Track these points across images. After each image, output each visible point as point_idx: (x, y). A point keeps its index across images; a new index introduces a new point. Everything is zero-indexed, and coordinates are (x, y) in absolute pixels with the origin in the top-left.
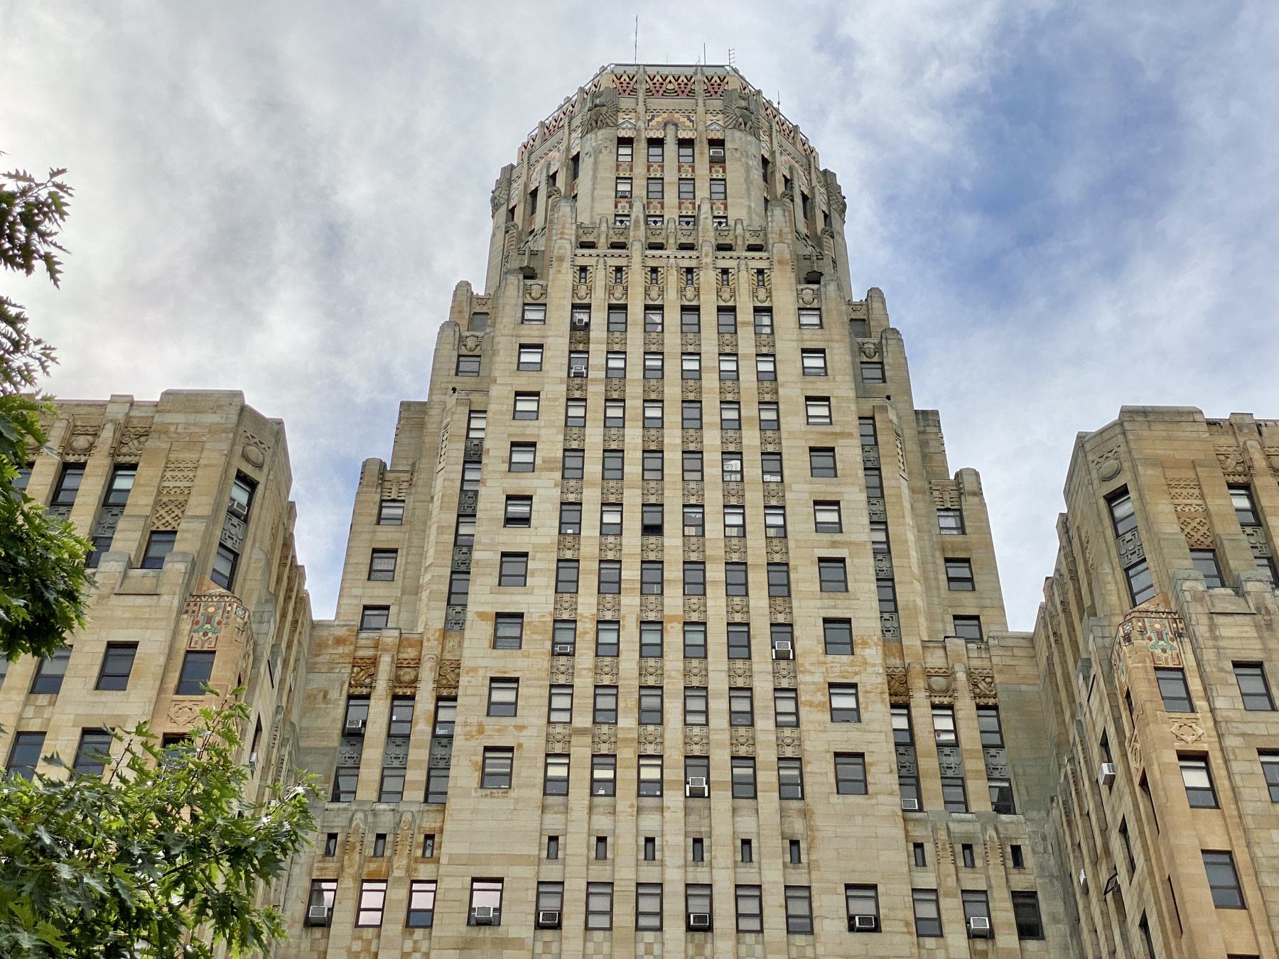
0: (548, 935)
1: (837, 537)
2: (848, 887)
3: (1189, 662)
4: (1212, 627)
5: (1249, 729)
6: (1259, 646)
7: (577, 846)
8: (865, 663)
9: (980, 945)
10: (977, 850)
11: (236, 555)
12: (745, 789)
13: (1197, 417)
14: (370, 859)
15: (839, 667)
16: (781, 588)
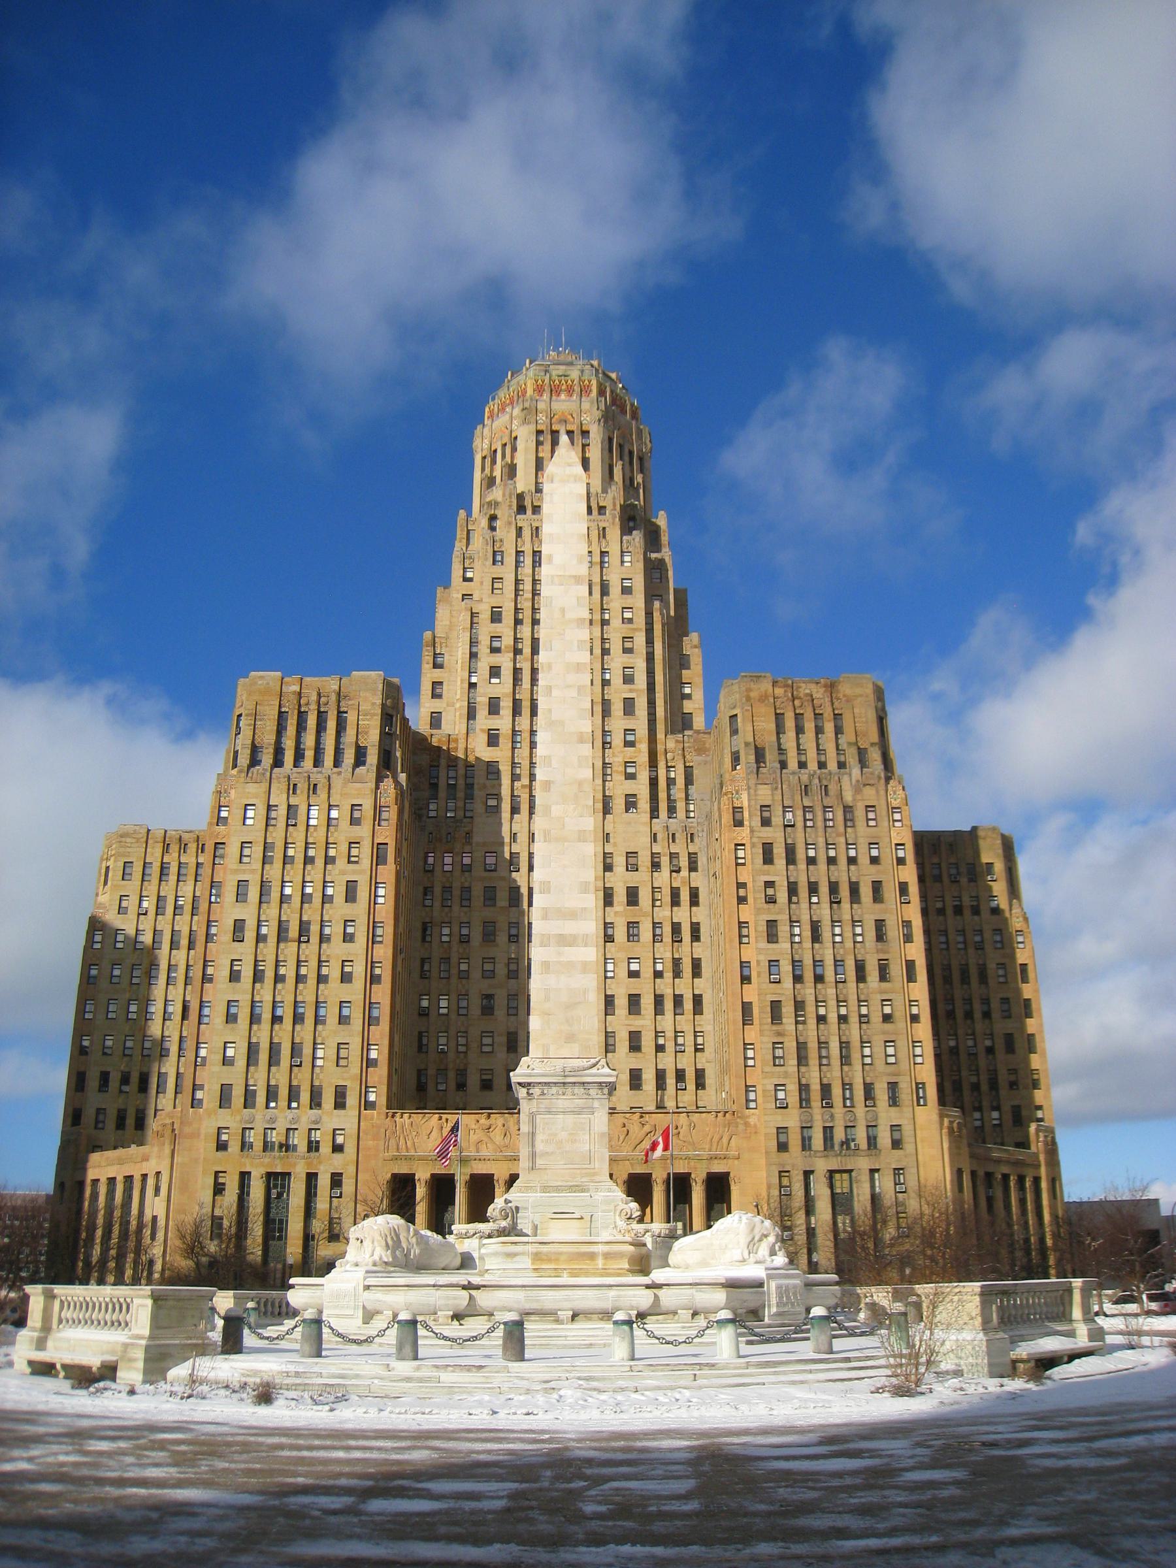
2: (627, 853)
3: (745, 804)
5: (761, 835)
6: (770, 797)
8: (640, 751)
10: (677, 835)
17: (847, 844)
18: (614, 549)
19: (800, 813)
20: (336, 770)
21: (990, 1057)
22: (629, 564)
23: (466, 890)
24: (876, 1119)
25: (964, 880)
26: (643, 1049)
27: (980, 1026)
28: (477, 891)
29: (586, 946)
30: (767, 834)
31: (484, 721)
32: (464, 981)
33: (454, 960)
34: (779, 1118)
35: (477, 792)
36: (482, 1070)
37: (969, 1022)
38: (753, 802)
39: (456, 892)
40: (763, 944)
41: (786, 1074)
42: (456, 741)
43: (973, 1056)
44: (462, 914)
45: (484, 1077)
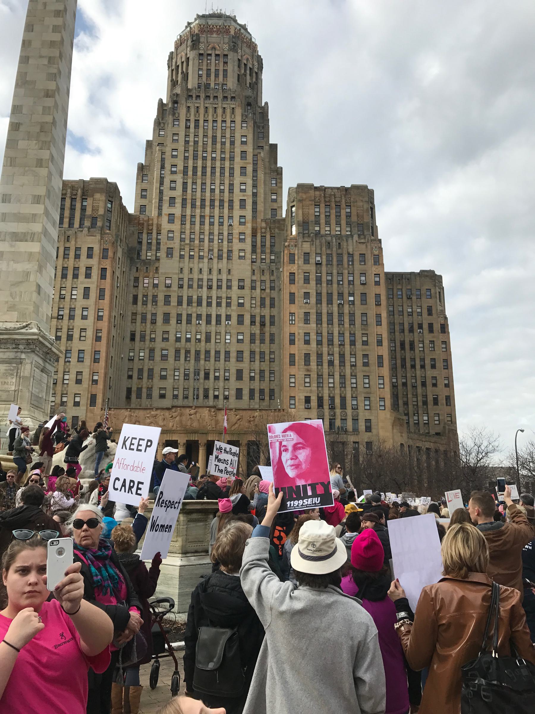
0: (181, 289)
1: (245, 193)
3: (296, 252)
4: (302, 245)
5: (303, 268)
6: (309, 249)
7: (186, 271)
8: (247, 228)
9: (263, 291)
10: (265, 271)
11: (110, 221)
12: (220, 257)
13: (313, 187)
14: (145, 273)
15: (242, 228)
16: (231, 207)
17: (349, 274)
18: (238, 119)
19: (324, 257)
20: (80, 229)
21: (424, 388)
22: (245, 128)
23: (155, 297)
24: (358, 416)
25: (414, 298)
26: (244, 379)
27: (419, 372)
28: (161, 298)
29: (32, 241)
30: (307, 267)
31: (166, 210)
32: (153, 343)
33: (148, 332)
34: (307, 413)
35: (162, 246)
36: (160, 388)
37: (413, 370)
38: (300, 251)
39: (150, 298)
40: (302, 325)
41: (311, 391)
42: (153, 220)
43: (414, 387)
44: (153, 309)
45: (162, 392)
